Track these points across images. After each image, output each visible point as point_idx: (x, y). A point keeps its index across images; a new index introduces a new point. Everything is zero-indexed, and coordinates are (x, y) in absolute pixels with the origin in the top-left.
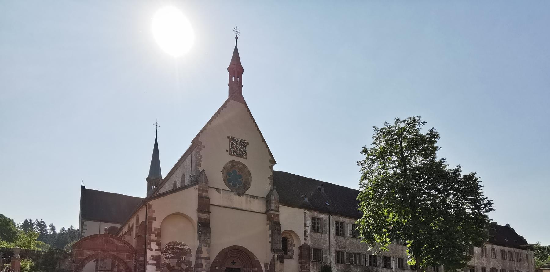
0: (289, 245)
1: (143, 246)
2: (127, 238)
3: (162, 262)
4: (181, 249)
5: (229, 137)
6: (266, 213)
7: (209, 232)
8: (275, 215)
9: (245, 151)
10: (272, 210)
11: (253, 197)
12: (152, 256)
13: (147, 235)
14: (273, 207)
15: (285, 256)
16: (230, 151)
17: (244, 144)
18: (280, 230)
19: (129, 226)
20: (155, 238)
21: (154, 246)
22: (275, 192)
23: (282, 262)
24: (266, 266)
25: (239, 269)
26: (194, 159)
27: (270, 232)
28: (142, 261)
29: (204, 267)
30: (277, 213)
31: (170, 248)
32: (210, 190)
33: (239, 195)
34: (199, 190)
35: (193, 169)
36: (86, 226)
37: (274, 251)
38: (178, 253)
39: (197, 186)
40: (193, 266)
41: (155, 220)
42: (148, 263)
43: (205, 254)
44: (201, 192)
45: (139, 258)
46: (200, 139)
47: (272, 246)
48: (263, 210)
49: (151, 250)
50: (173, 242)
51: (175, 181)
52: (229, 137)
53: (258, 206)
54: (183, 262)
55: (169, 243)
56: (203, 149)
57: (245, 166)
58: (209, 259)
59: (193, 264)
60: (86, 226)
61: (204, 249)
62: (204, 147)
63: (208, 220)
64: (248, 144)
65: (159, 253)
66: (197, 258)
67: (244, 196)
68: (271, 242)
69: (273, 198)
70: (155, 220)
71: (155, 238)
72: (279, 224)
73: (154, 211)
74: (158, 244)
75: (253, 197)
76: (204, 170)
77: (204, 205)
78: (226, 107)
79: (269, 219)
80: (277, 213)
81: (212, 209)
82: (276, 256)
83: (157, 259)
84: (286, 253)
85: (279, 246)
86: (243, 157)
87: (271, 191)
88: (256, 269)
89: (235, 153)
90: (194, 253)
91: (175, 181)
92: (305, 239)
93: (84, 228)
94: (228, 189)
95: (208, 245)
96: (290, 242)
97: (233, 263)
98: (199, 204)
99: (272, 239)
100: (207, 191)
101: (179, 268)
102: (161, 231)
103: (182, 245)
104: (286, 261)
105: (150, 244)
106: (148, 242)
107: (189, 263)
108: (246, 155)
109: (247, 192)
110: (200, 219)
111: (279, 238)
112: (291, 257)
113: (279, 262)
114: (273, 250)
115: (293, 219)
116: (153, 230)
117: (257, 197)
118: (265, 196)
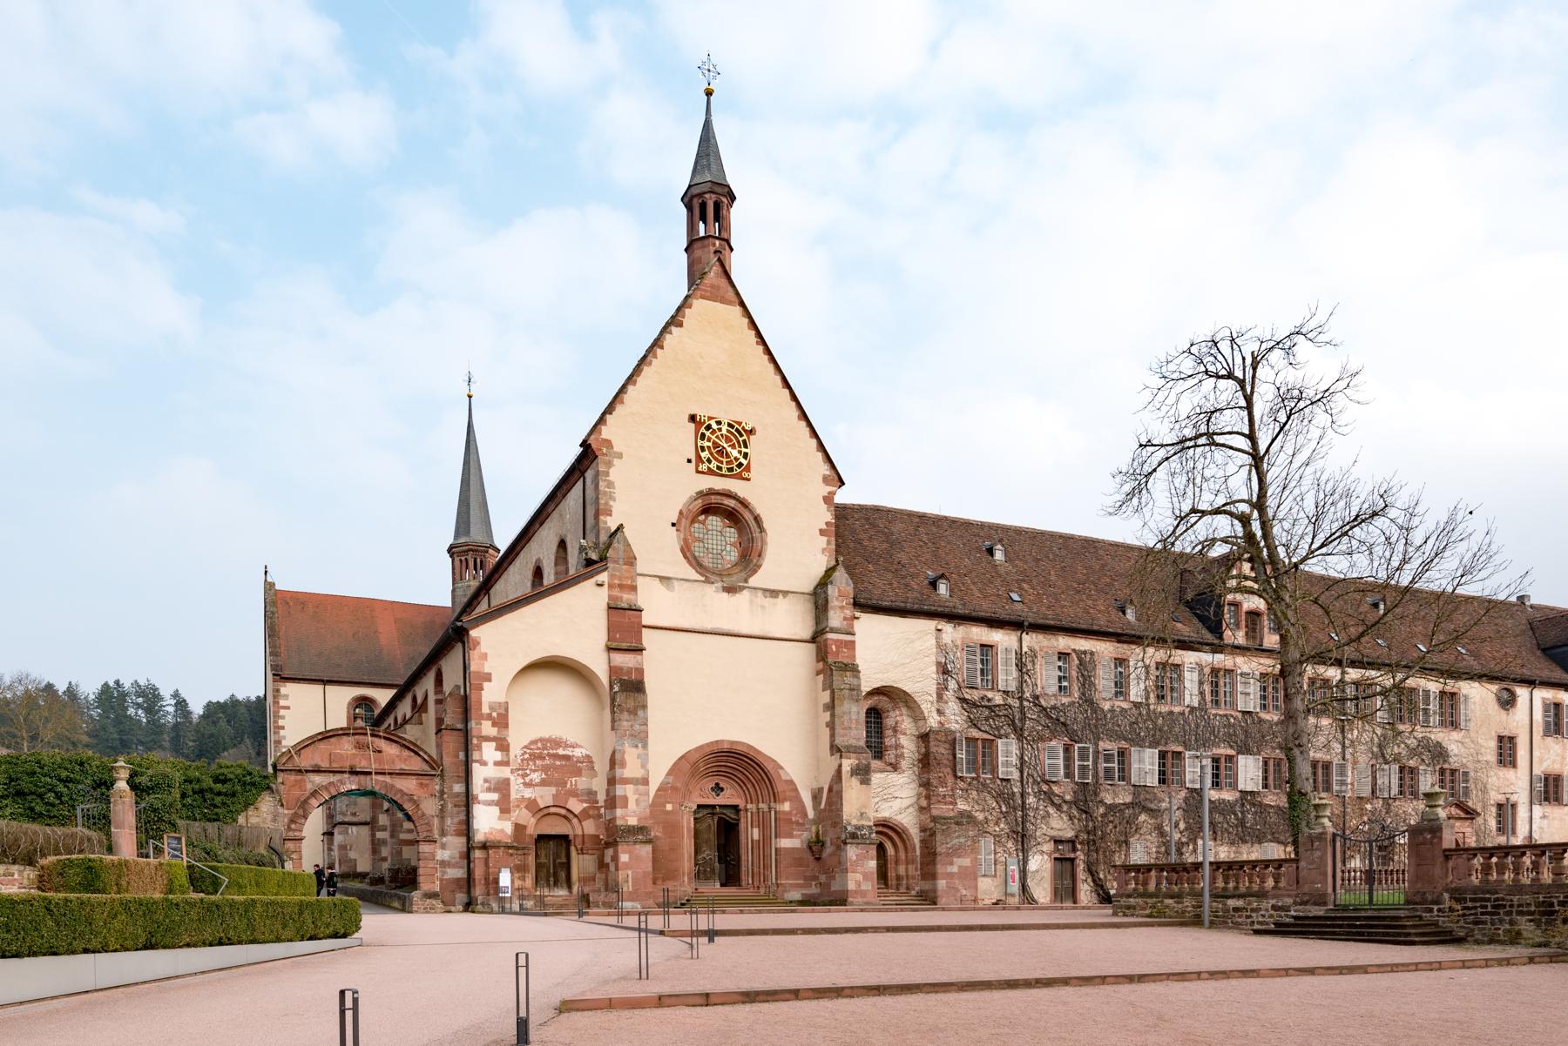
0: (889, 732)
1: (462, 755)
2: (411, 732)
3: (514, 795)
4: (567, 758)
5: (693, 418)
6: (813, 640)
7: (644, 707)
8: (839, 643)
9: (746, 456)
10: (833, 631)
11: (774, 593)
12: (486, 781)
13: (472, 724)
14: (835, 619)
15: (875, 764)
16: (699, 459)
17: (741, 434)
18: (855, 689)
19: (414, 699)
20: (493, 732)
21: (489, 752)
22: (841, 575)
23: (866, 781)
24: (816, 797)
25: (735, 808)
26: (590, 492)
27: (826, 697)
28: (458, 795)
29: (632, 805)
30: (849, 638)
31: (534, 757)
32: (640, 581)
33: (730, 590)
34: (611, 586)
35: (588, 526)
36: (286, 697)
37: (839, 750)
38: (556, 768)
39: (603, 577)
40: (601, 803)
41: (489, 680)
42: (475, 798)
43: (631, 770)
44: (616, 592)
45: (451, 788)
46: (605, 432)
47: (832, 736)
48: (805, 629)
49: (484, 763)
50: (541, 740)
51: (538, 560)
52: (693, 418)
53: (793, 619)
54: (574, 793)
55: (532, 742)
56: (616, 461)
57: (744, 504)
58: (645, 781)
59: (601, 797)
60: (286, 697)
61: (631, 754)
62: (620, 456)
63: (640, 671)
64: (751, 432)
65: (505, 772)
66: (612, 781)
67: (745, 592)
68: (831, 725)
69: (832, 591)
70: (489, 680)
71: (493, 732)
72: (853, 669)
73: (484, 657)
74: (503, 746)
75: (774, 593)
76: (620, 528)
77: (625, 628)
78: (681, 325)
79: (822, 655)
80: (849, 638)
81: (648, 637)
82: (847, 764)
83: (502, 787)
84: (879, 754)
85: (856, 734)
86: (739, 477)
87: (830, 572)
88: (786, 807)
89: (714, 465)
90: (602, 767)
91: (538, 560)
92: (939, 712)
93: (282, 703)
94: (695, 576)
95: (641, 739)
96: (889, 722)
97: (718, 789)
98: (612, 629)
99: (833, 716)
100: (634, 588)
101: (563, 812)
102: (507, 710)
103: (567, 746)
104: (876, 778)
105: (479, 748)
106: (475, 741)
107: (591, 794)
108: (748, 469)
109: (753, 581)
110: (613, 671)
111: (854, 715)
112: (895, 767)
113: (855, 782)
114: (835, 749)
115: (895, 651)
116: (485, 710)
117: (786, 593)
118: (808, 586)
